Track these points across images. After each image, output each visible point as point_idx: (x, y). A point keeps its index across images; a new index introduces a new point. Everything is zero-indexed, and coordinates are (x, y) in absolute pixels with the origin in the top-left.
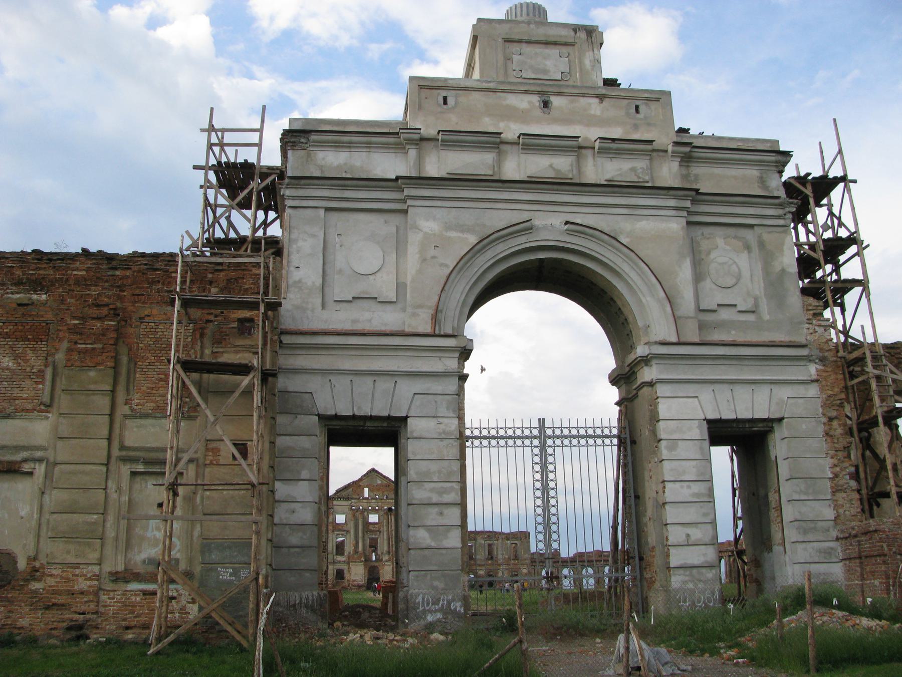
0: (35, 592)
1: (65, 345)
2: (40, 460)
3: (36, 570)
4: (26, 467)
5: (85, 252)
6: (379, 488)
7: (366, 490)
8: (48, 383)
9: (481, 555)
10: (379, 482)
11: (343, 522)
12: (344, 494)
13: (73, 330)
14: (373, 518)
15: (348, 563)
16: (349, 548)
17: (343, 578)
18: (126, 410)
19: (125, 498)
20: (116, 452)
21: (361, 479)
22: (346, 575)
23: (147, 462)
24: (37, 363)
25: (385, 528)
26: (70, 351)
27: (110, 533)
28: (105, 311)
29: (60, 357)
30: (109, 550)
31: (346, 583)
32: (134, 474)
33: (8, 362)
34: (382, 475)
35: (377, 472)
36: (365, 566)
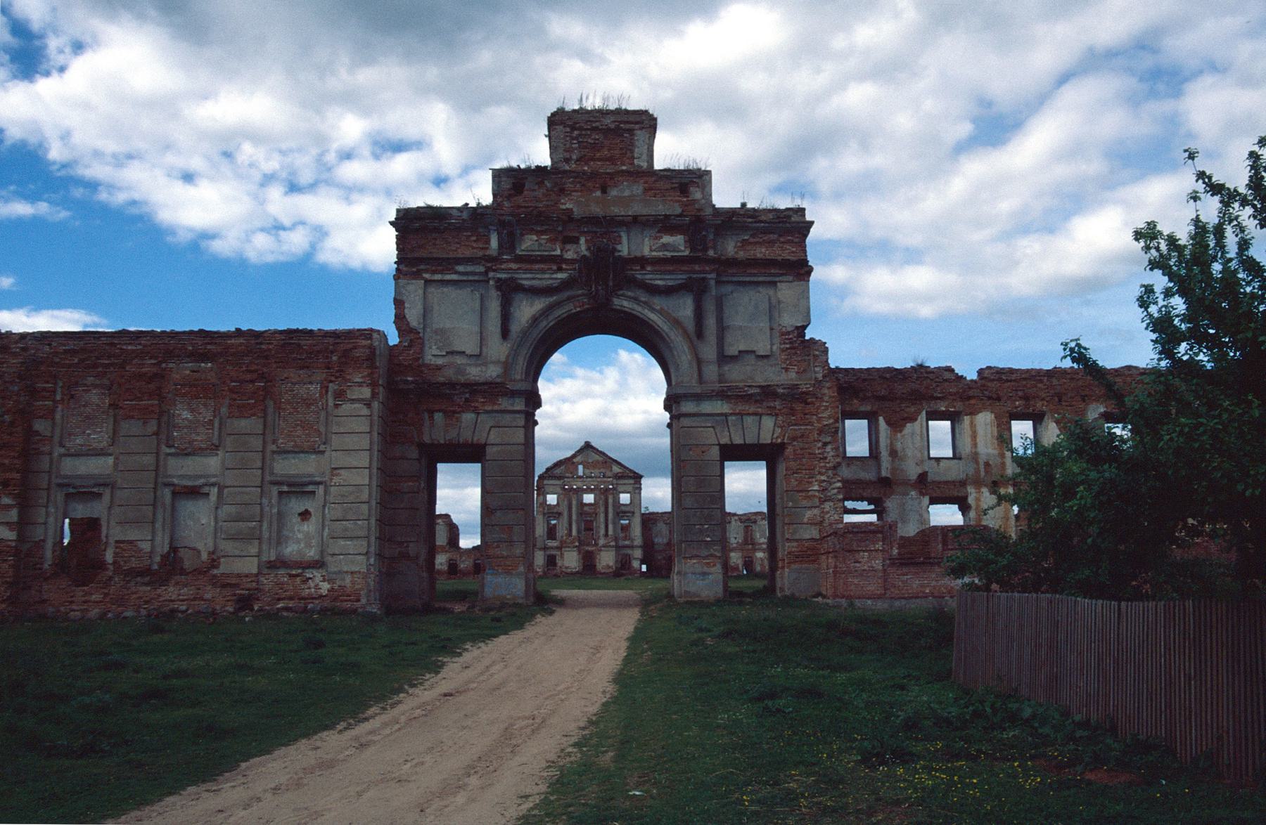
0: (215, 576)
1: (227, 401)
2: (213, 485)
3: (213, 560)
4: (206, 490)
5: (238, 330)
6: (595, 465)
7: (581, 467)
8: (216, 430)
12: (558, 471)
13: (232, 391)
14: (589, 498)
16: (561, 532)
17: (555, 564)
18: (274, 448)
19: (275, 510)
20: (268, 478)
21: (574, 456)
22: (559, 563)
23: (289, 485)
24: (207, 415)
25: (602, 509)
26: (230, 405)
27: (266, 535)
28: (255, 376)
29: (224, 410)
30: (265, 547)
31: (558, 570)
32: (281, 493)
33: (186, 414)
36: (579, 552)
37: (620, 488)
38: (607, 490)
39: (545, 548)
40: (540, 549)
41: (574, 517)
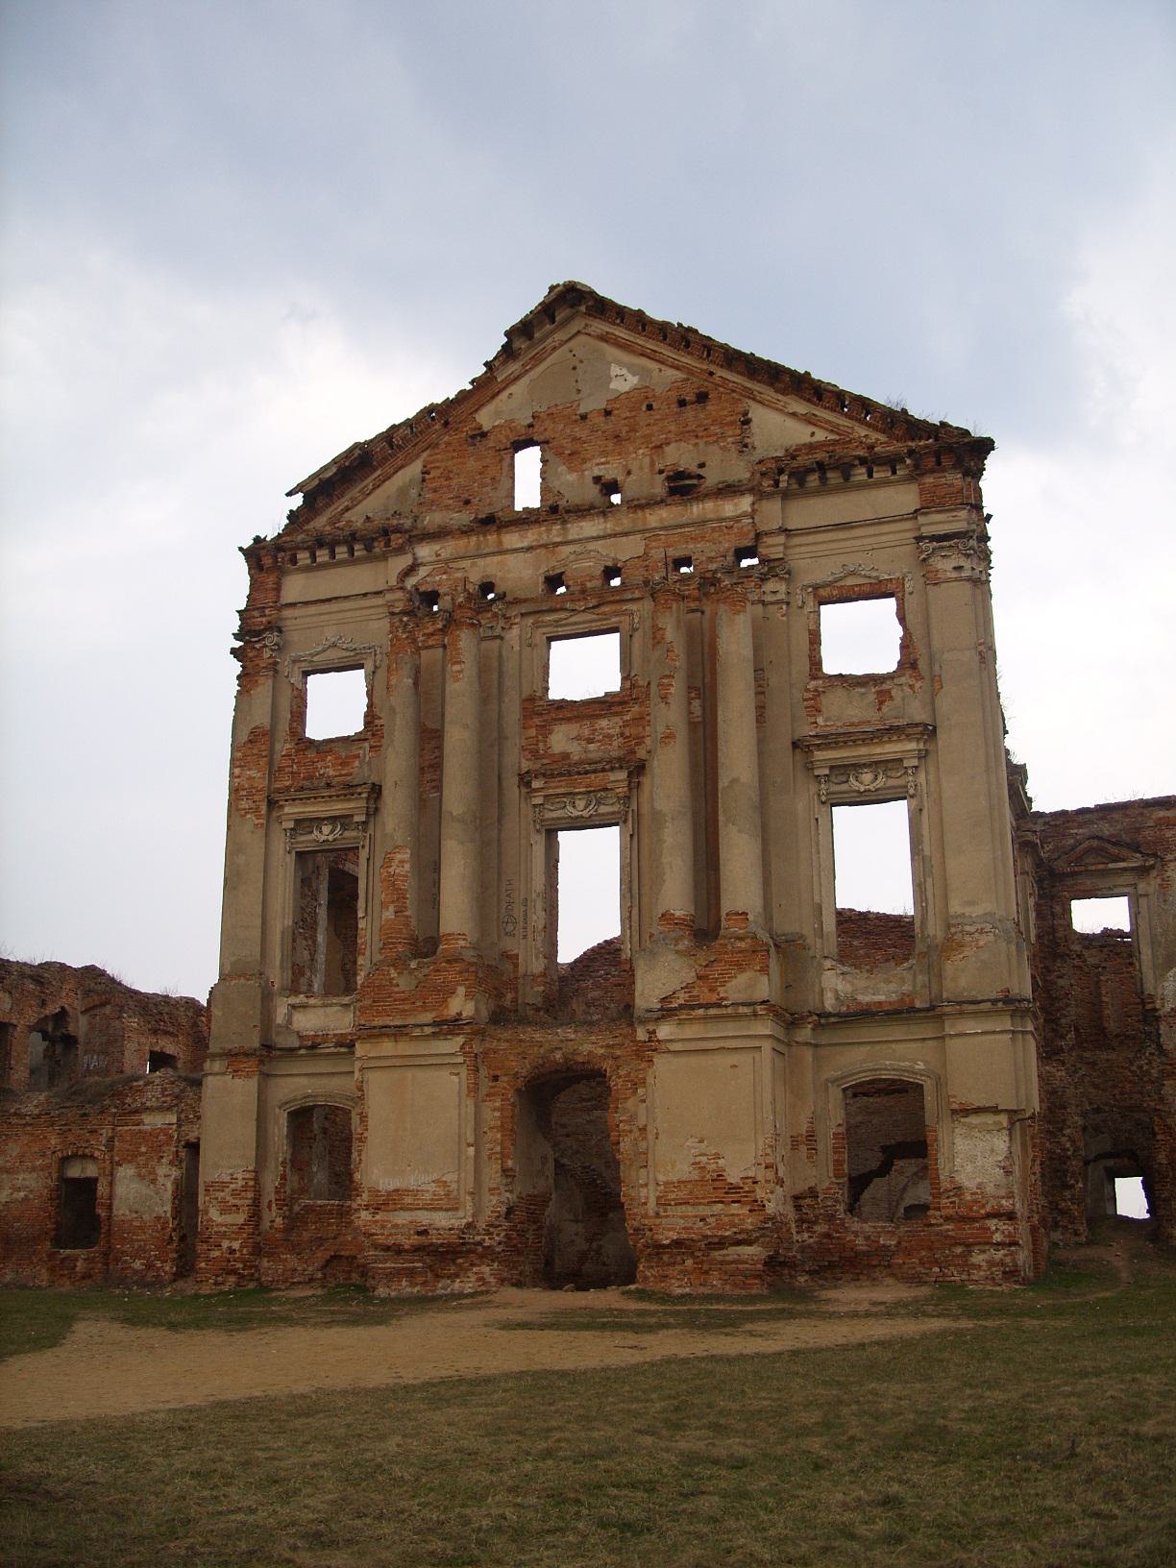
6: (622, 421)
7: (528, 463)
10: (623, 379)
11: (352, 723)
12: (369, 506)
14: (585, 667)
17: (343, 1182)
21: (485, 387)
34: (638, 321)
35: (604, 308)
37: (813, 564)
39: (268, 1054)
40: (234, 1057)
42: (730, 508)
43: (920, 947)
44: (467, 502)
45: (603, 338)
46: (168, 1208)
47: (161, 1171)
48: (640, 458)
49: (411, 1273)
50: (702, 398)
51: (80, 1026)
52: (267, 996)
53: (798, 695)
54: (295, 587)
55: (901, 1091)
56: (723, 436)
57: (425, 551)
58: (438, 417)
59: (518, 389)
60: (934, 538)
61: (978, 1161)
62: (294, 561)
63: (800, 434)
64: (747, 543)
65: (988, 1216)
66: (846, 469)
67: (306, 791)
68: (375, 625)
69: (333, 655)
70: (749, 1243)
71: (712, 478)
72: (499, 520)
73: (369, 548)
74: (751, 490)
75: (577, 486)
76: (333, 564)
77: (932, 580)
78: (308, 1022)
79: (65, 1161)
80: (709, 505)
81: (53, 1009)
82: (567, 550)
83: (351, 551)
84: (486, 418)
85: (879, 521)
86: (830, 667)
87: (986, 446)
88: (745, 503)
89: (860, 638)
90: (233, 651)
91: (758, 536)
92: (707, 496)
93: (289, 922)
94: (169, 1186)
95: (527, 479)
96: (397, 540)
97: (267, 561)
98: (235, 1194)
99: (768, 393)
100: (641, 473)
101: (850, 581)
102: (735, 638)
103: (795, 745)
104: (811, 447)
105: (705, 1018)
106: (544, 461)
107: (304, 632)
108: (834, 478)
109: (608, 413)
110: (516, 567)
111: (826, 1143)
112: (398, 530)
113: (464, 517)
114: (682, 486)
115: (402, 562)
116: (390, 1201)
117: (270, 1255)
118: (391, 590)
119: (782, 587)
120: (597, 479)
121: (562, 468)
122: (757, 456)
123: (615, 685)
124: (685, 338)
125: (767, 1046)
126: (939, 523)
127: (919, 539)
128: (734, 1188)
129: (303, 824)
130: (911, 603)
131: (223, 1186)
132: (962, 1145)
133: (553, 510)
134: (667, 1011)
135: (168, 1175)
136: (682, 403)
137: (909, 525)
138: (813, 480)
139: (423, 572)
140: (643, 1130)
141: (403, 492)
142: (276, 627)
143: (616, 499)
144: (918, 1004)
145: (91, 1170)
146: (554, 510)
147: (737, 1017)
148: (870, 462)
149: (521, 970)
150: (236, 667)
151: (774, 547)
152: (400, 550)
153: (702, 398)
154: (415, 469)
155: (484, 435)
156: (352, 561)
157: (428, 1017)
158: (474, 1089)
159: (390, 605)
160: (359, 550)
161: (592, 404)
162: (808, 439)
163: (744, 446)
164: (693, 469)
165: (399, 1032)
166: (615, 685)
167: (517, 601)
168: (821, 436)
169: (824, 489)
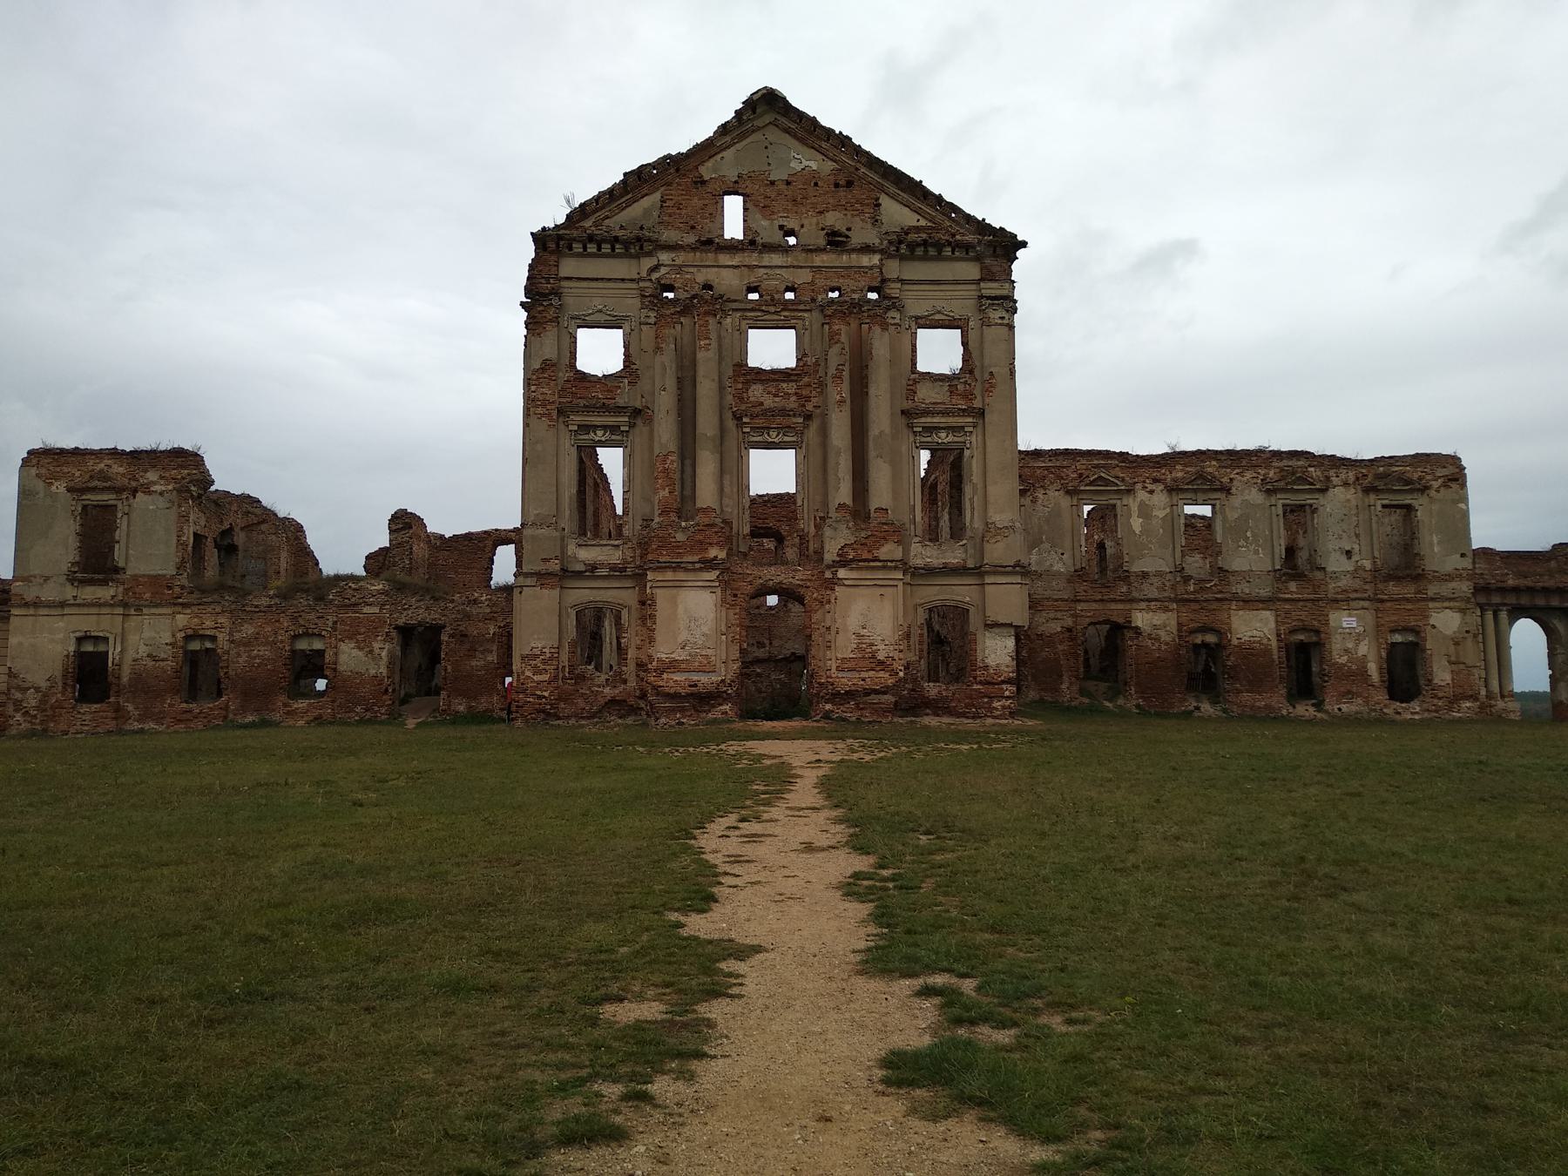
6: (798, 192)
7: (733, 207)
9: (1251, 559)
14: (772, 349)
15: (640, 578)
21: (704, 150)
22: (631, 639)
25: (839, 391)
38: (852, 308)
41: (707, 422)
42: (866, 260)
43: (969, 533)
44: (693, 227)
45: (787, 131)
46: (383, 670)
47: (376, 645)
48: (811, 221)
49: (682, 710)
50: (849, 184)
51: (240, 538)
52: (562, 539)
53: (904, 382)
54: (569, 267)
55: (961, 613)
56: (863, 212)
57: (665, 257)
58: (671, 165)
59: (729, 154)
60: (989, 298)
61: (997, 652)
62: (570, 248)
63: (909, 218)
64: (875, 284)
65: (1003, 682)
66: (939, 246)
67: (589, 409)
68: (630, 301)
69: (602, 318)
70: (885, 693)
71: (857, 239)
72: (714, 244)
73: (627, 249)
74: (882, 252)
75: (768, 230)
76: (599, 255)
77: (985, 323)
78: (587, 555)
79: (296, 637)
80: (854, 256)
81: (226, 526)
82: (763, 271)
83: (613, 249)
84: (706, 171)
85: (956, 282)
86: (921, 367)
87: (1024, 244)
88: (876, 259)
89: (939, 352)
90: (522, 304)
91: (884, 281)
92: (854, 250)
93: (574, 491)
94: (384, 654)
95: (733, 218)
96: (648, 247)
97: (552, 246)
98: (544, 662)
99: (893, 189)
100: (811, 229)
101: (937, 317)
102: (880, 345)
103: (903, 412)
104: (918, 229)
105: (867, 568)
106: (745, 209)
107: (574, 298)
108: (932, 252)
109: (788, 183)
110: (727, 279)
111: (914, 639)
112: (649, 240)
113: (691, 239)
114: (836, 240)
115: (648, 263)
116: (673, 666)
117: (565, 701)
118: (641, 279)
119: (898, 316)
120: (781, 227)
121: (758, 216)
122: (884, 230)
123: (793, 364)
124: (844, 141)
125: (900, 584)
126: (991, 289)
127: (981, 297)
128: (881, 663)
129: (586, 428)
130: (972, 335)
131: (536, 657)
132: (988, 643)
133: (750, 243)
134: (843, 562)
135: (384, 649)
136: (837, 185)
137: (974, 287)
138: (919, 251)
139: (663, 270)
140: (828, 629)
141: (647, 212)
142: (557, 293)
143: (792, 241)
144: (970, 564)
145: (318, 645)
146: (753, 243)
147: (884, 567)
148: (956, 246)
149: (735, 530)
150: (524, 315)
151: (893, 290)
152: (650, 254)
153: (849, 184)
154: (657, 196)
155: (703, 182)
156: (613, 255)
157: (696, 558)
158: (724, 601)
159: (642, 289)
160: (619, 249)
161: (778, 175)
162: (915, 224)
163: (876, 221)
164: (844, 230)
165: (677, 567)
166: (793, 364)
167: (729, 300)
168: (923, 223)
169: (925, 258)
